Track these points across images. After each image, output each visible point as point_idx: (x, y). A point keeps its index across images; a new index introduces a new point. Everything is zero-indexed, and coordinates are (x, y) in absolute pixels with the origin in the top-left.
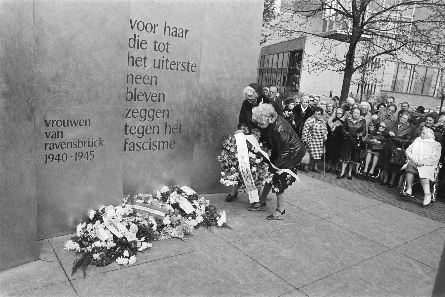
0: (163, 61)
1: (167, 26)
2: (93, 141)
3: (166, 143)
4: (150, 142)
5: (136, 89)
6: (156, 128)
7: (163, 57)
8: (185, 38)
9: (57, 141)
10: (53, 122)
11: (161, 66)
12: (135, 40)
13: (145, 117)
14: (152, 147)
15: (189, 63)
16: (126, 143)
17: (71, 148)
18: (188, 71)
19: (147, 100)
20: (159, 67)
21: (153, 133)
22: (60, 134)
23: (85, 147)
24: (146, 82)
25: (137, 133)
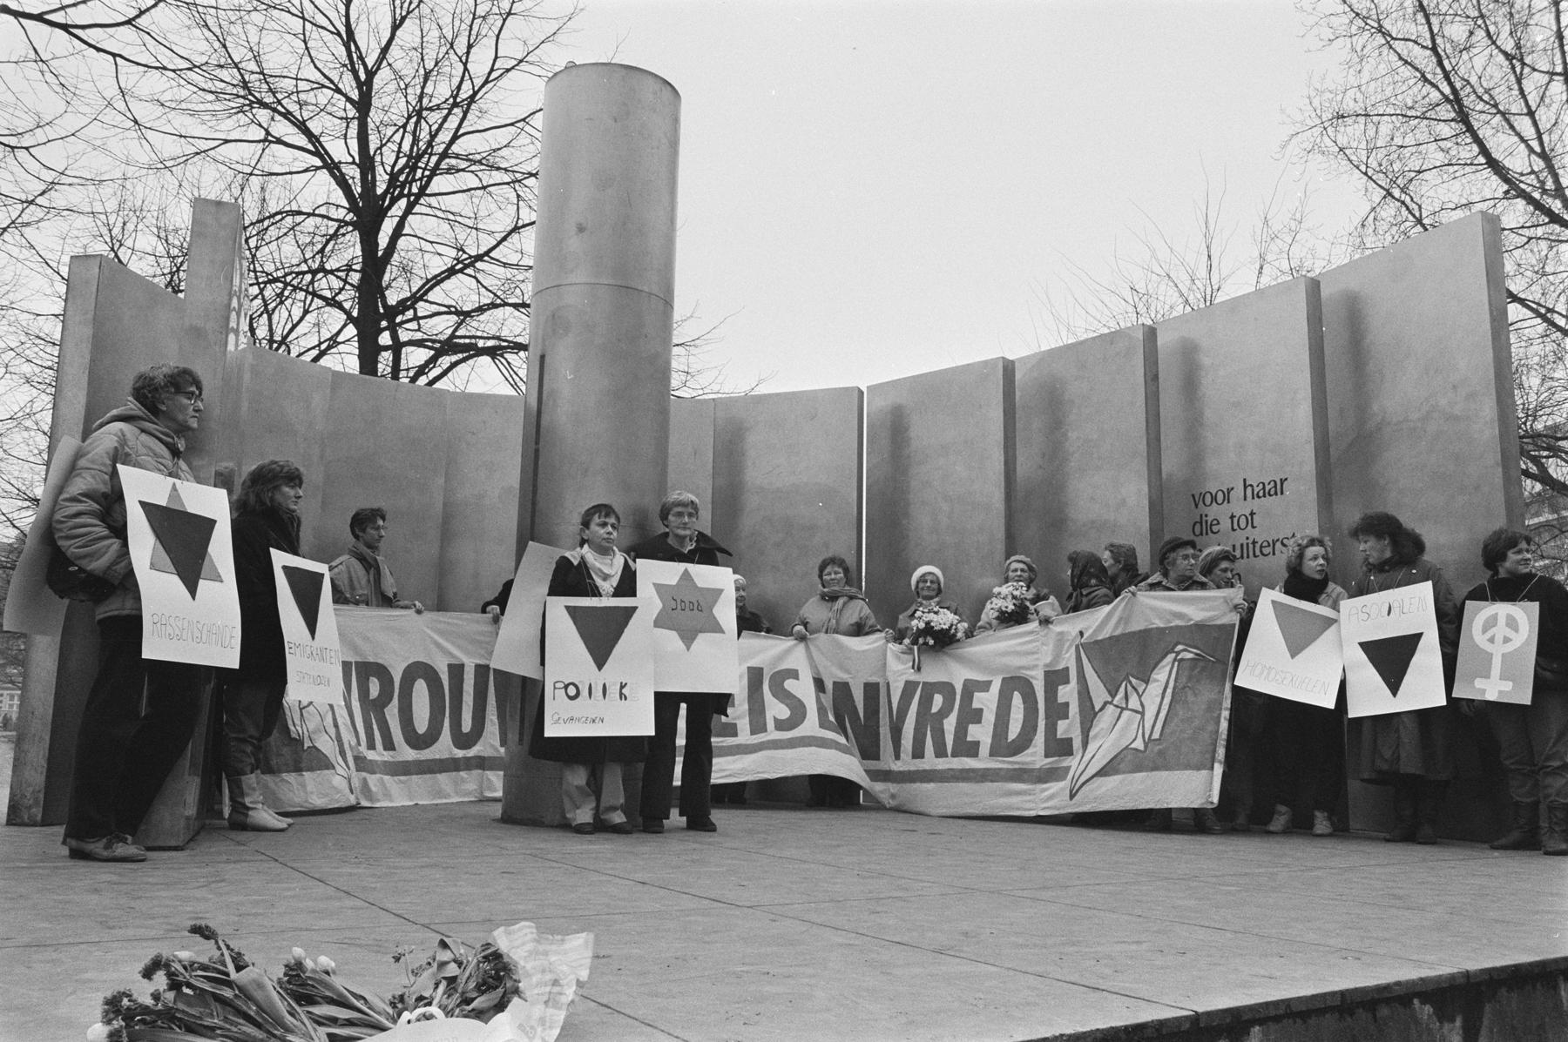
0: (1247, 544)
7: (1247, 538)
11: (1245, 555)
20: (1242, 557)
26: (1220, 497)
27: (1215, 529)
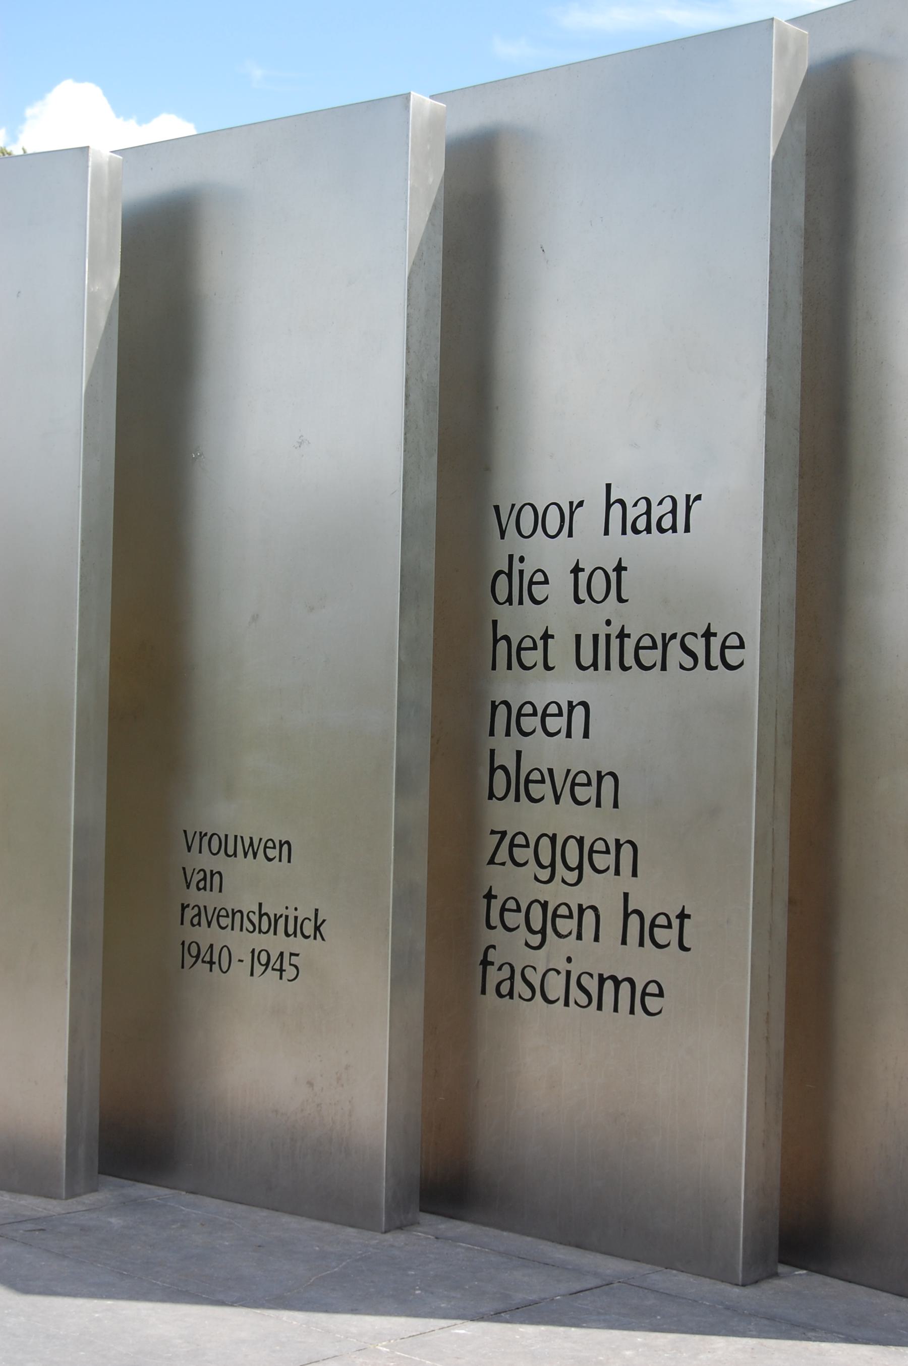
0: (608, 636)
2: (296, 918)
4: (568, 973)
5: (519, 753)
7: (608, 623)
8: (687, 529)
12: (510, 575)
14: (575, 991)
15: (708, 635)
17: (241, 930)
18: (709, 667)
23: (275, 933)
24: (551, 730)
27: (539, 592)
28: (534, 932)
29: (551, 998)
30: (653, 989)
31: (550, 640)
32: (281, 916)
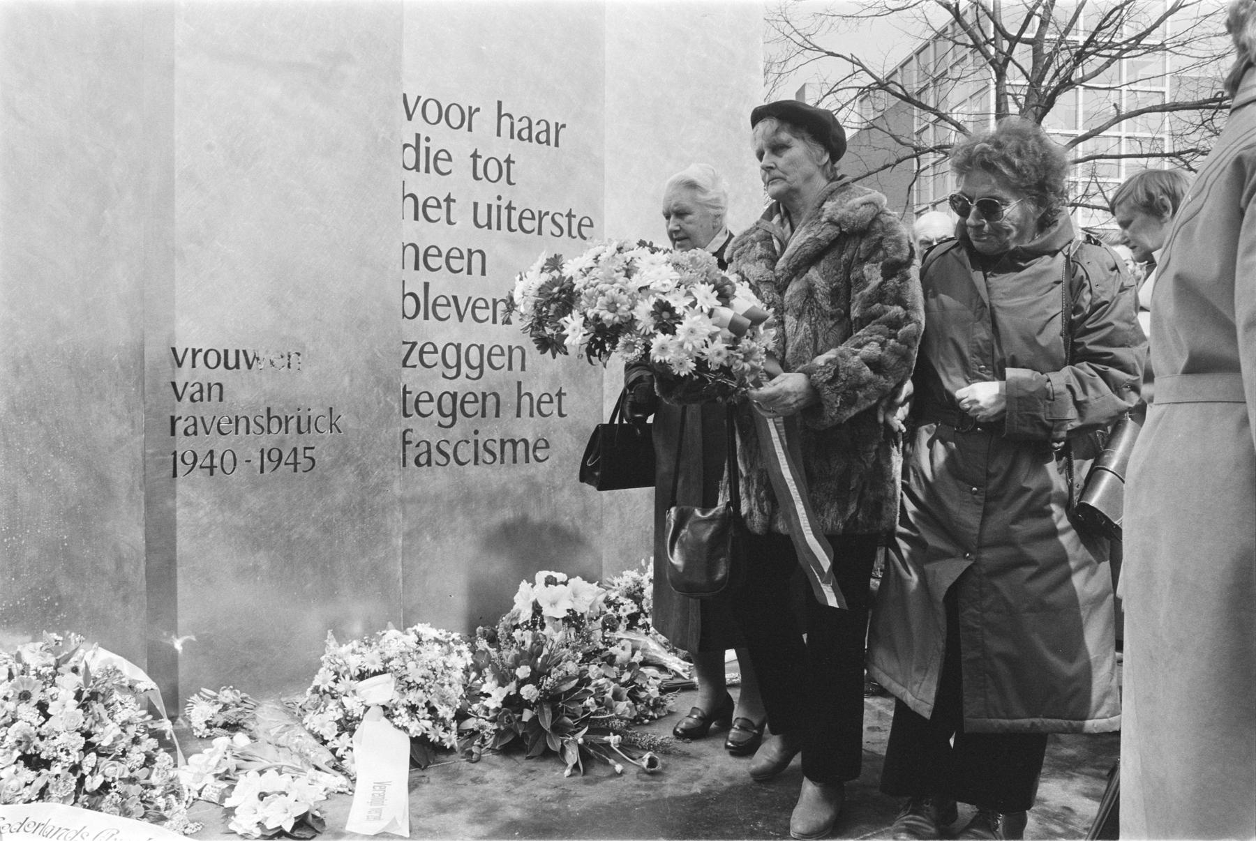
0: (499, 207)
1: (503, 113)
2: (309, 417)
3: (521, 446)
4: (476, 441)
5: (426, 285)
6: (491, 401)
7: (499, 198)
8: (557, 145)
9: (206, 410)
10: (194, 353)
12: (417, 149)
13: (458, 365)
15: (570, 215)
16: (405, 443)
17: (248, 432)
19: (461, 318)
21: (484, 415)
22: (216, 390)
23: (287, 432)
24: (455, 267)
25: (436, 413)
26: (455, 118)
27: (443, 166)
28: (445, 416)
29: (463, 460)
30: (542, 444)
31: (452, 204)
32: (292, 417)
